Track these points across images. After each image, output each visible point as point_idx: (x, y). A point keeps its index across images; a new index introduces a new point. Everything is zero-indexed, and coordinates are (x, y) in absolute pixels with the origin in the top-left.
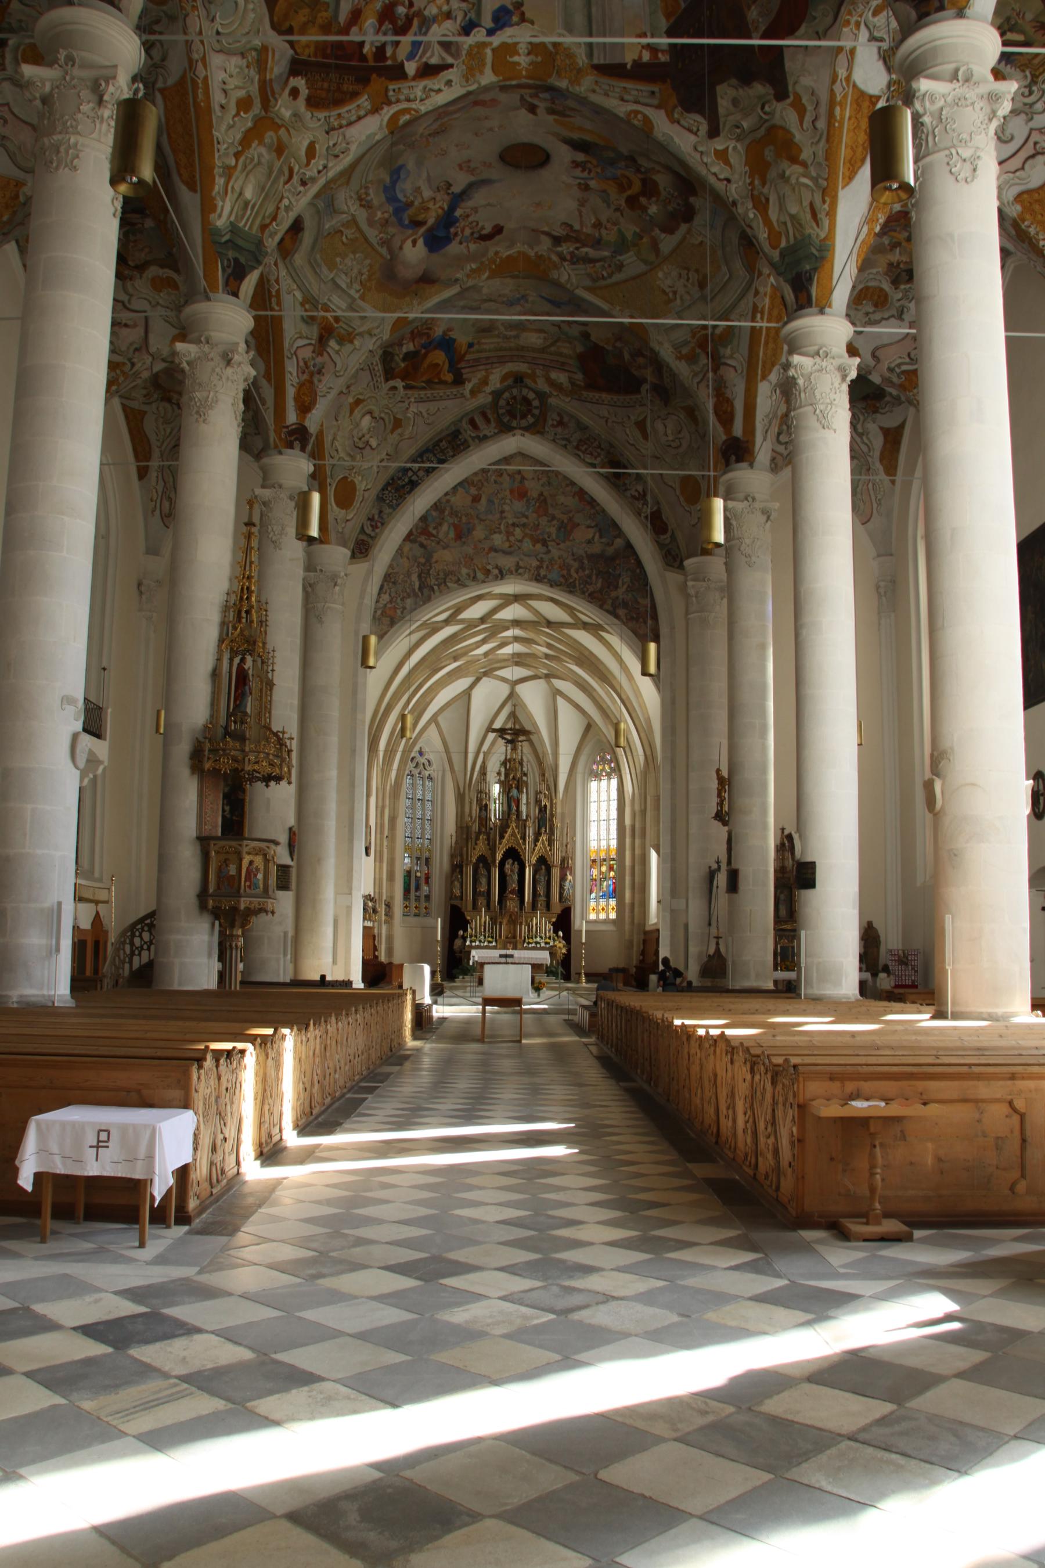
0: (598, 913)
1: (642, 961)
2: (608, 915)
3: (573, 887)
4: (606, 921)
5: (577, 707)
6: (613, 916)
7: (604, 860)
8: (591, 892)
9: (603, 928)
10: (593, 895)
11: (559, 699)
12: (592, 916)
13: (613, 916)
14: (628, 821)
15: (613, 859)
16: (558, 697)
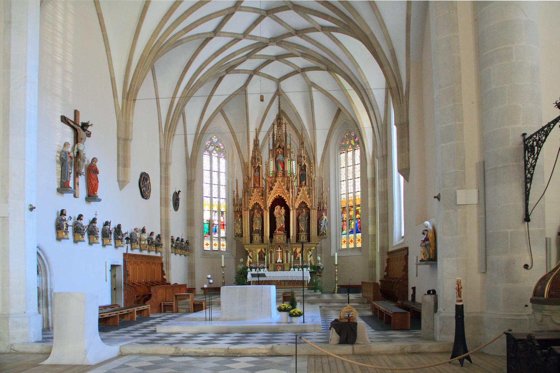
0: (348, 244)
1: (385, 277)
2: (355, 244)
3: (329, 227)
4: (355, 248)
5: (327, 94)
6: (359, 245)
7: (352, 207)
8: (343, 230)
9: (349, 253)
10: (344, 232)
11: (313, 89)
12: (344, 246)
13: (359, 245)
14: (369, 175)
15: (359, 206)
16: (313, 89)
